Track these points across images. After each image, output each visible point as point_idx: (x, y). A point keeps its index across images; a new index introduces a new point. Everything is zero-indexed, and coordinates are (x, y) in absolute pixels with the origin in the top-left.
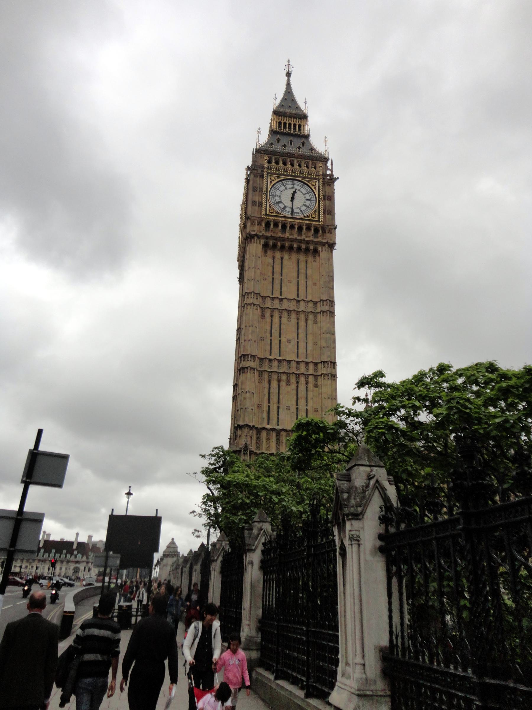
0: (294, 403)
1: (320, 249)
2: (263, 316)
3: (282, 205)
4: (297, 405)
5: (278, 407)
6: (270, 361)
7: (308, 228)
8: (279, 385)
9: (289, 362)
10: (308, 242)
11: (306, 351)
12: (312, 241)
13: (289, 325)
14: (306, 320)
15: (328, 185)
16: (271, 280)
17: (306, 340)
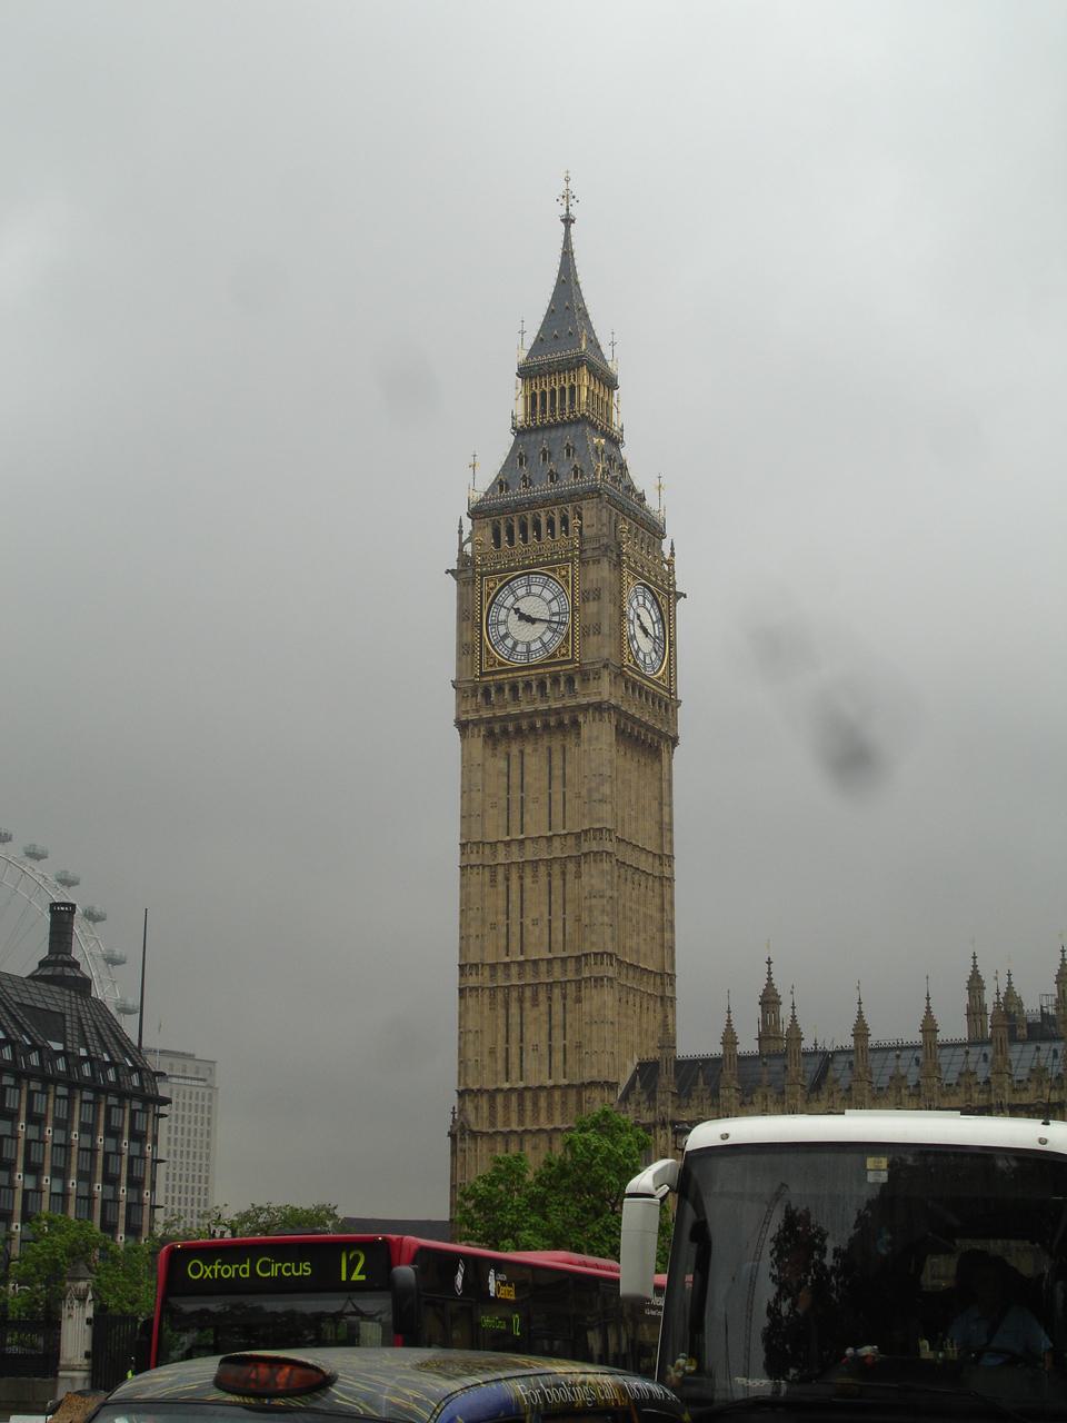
0: (544, 1037)
1: (581, 719)
2: (493, 881)
3: (510, 643)
4: (550, 1040)
5: (521, 1048)
6: (507, 965)
7: (556, 681)
8: (521, 1009)
9: (535, 962)
10: (557, 712)
11: (564, 935)
12: (564, 708)
13: (535, 890)
14: (564, 873)
15: (594, 562)
16: (504, 803)
17: (564, 913)
